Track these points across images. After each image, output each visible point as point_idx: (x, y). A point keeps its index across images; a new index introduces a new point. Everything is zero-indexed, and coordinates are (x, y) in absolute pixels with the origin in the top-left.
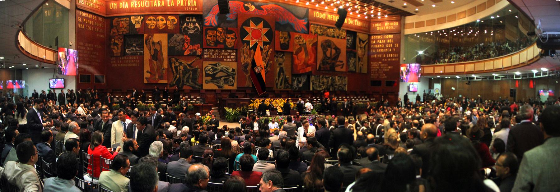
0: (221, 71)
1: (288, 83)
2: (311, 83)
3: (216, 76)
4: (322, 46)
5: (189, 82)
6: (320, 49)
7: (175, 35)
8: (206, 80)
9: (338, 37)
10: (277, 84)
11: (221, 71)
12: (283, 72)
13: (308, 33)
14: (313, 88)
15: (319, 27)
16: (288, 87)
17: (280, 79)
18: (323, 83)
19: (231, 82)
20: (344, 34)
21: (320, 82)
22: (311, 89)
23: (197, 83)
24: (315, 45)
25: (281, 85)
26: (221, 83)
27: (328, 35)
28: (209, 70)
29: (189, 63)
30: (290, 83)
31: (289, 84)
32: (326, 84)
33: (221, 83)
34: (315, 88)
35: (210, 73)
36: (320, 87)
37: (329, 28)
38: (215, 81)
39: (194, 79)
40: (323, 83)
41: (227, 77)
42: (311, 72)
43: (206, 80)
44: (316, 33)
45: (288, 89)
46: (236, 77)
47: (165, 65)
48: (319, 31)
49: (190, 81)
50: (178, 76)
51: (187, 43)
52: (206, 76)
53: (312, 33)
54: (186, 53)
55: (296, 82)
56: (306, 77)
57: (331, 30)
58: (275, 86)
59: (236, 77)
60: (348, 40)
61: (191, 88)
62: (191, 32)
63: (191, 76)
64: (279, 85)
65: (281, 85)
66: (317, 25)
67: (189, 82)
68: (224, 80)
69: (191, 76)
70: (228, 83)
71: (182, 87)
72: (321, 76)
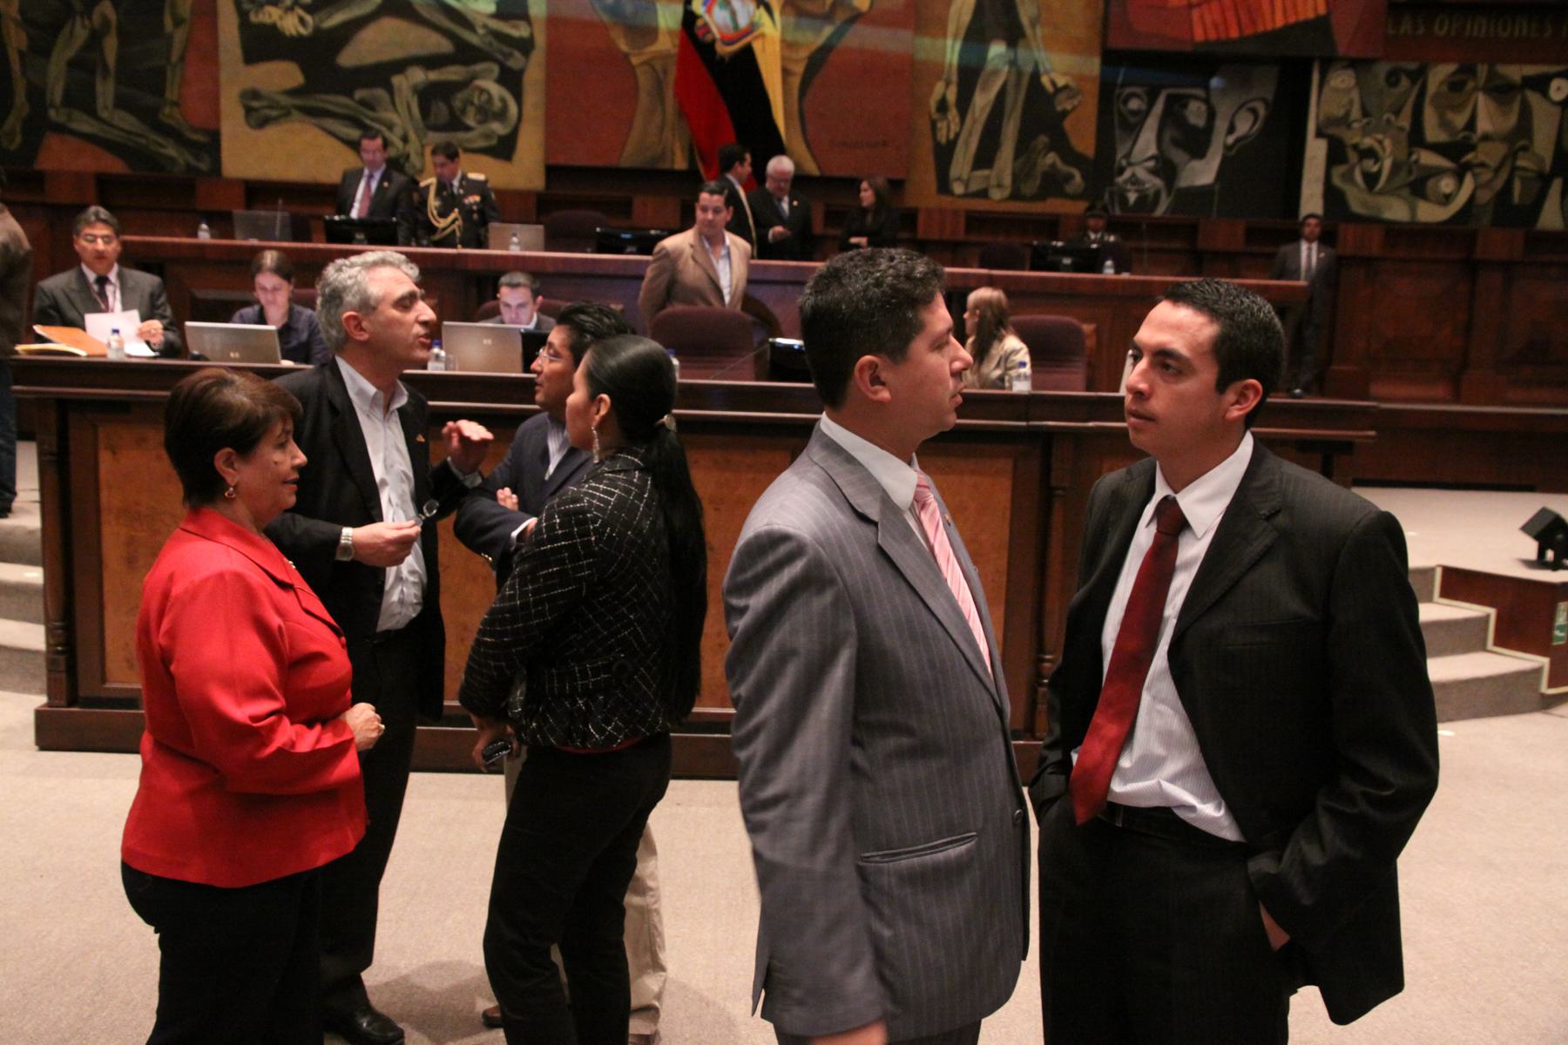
1: (1060, 143)
2: (1316, 151)
5: (91, 111)
10: (944, 154)
12: (1014, 36)
14: (1332, 196)
16: (1053, 185)
17: (982, 101)
18: (1457, 150)
19: (486, 114)
21: (1416, 137)
23: (168, 114)
25: (984, 159)
30: (1084, 140)
32: (1490, 154)
34: (1357, 200)
35: (291, 24)
36: (1418, 188)
38: (337, 102)
39: (144, 85)
40: (1457, 150)
41: (452, 73)
42: (1320, 26)
43: (254, 94)
45: (1054, 206)
46: (534, 74)
49: (105, 91)
55: (1147, 143)
56: (1265, 88)
58: (931, 178)
59: (534, 74)
61: (115, 165)
63: (111, 45)
65: (984, 159)
67: (91, 111)
68: (427, 95)
69: (111, 45)
70: (455, 124)
71: (32, 145)
72: (1439, 74)
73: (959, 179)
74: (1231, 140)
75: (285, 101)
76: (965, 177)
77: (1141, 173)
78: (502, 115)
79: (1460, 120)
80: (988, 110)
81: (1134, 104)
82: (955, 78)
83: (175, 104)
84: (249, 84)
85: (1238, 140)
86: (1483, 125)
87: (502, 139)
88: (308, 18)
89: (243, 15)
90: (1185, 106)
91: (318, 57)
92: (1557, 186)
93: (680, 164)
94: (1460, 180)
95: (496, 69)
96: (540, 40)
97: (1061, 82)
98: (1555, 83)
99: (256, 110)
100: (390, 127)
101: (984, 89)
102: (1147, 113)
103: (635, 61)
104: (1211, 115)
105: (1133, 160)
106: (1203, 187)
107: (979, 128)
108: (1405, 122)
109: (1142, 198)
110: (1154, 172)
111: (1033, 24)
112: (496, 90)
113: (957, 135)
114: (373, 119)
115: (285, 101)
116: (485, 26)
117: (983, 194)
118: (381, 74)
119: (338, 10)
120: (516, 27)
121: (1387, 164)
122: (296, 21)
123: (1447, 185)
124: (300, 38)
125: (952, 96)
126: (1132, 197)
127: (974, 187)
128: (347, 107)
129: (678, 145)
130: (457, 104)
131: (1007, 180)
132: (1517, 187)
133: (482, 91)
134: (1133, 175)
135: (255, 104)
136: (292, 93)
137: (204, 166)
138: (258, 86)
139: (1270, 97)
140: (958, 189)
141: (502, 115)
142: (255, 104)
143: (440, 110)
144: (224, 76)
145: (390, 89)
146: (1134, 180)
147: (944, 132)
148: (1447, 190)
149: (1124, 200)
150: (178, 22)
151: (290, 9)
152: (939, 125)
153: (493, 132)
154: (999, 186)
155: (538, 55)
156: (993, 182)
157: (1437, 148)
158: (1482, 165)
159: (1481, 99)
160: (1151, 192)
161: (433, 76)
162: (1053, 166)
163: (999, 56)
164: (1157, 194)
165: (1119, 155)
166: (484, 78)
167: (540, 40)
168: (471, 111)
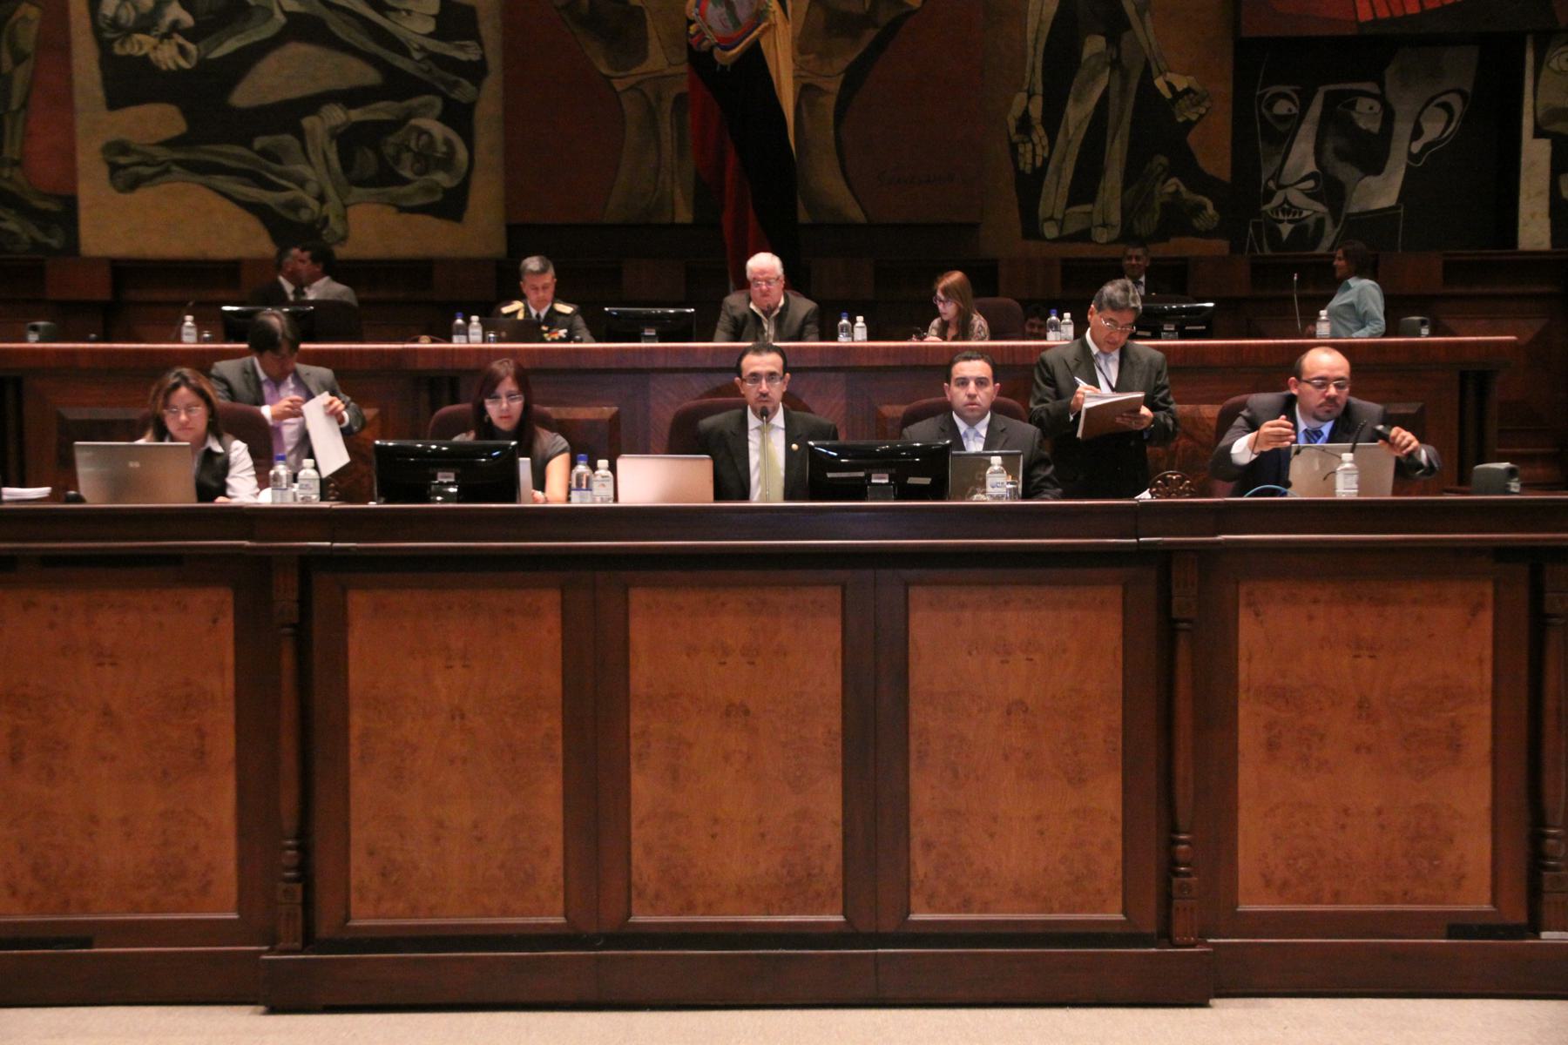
0: (302, 28)
1: (1184, 165)
3: (242, 97)
8: (116, 150)
10: (1030, 186)
11: (302, 28)
16: (1177, 220)
17: (1077, 114)
19: (427, 160)
25: (1084, 188)
26: (311, 173)
28: (146, 23)
30: (1216, 160)
31: (1200, 181)
33: (311, 173)
35: (167, 56)
41: (380, 111)
43: (122, 148)
46: (489, 102)
52: (116, 100)
55: (1302, 156)
59: (489, 102)
64: (1053, 198)
65: (1084, 188)
68: (349, 140)
70: (386, 177)
73: (1051, 218)
74: (1416, 147)
75: (163, 154)
76: (1059, 216)
77: (1296, 197)
78: (447, 163)
80: (1085, 126)
81: (1282, 107)
82: (1039, 88)
83: (16, 163)
84: (114, 135)
85: (1427, 146)
87: (446, 191)
88: (191, 47)
89: (104, 47)
90: (1352, 106)
91: (203, 95)
93: (684, 216)
95: (438, 103)
96: (494, 62)
97: (1181, 84)
99: (125, 167)
100: (302, 183)
101: (1077, 100)
102: (1300, 118)
103: (618, 86)
104: (1388, 117)
105: (1283, 181)
106: (1383, 217)
107: (1075, 150)
109: (1300, 230)
110: (1312, 195)
111: (1140, 13)
112: (438, 130)
113: (1046, 161)
114: (281, 175)
115: (163, 154)
116: (422, 49)
117: (1084, 236)
118: (287, 115)
119: (229, 37)
120: (462, 48)
122: (175, 51)
124: (180, 68)
125: (1036, 110)
126: (1286, 229)
127: (1071, 228)
128: (240, 158)
129: (678, 191)
130: (389, 150)
131: (1116, 217)
133: (422, 132)
134: (1286, 201)
135: (122, 160)
136: (170, 144)
137: (54, 243)
138: (125, 137)
139: (1468, 89)
140: (1051, 231)
141: (447, 163)
142: (122, 160)
143: (367, 161)
144: (81, 124)
145: (300, 134)
146: (1288, 208)
147: (1029, 156)
149: (1274, 234)
150: (19, 58)
151: (167, 36)
152: (1021, 150)
153: (438, 184)
154: (1104, 225)
155: (492, 85)
156: (1097, 219)
160: (1311, 222)
161: (356, 115)
162: (1177, 192)
163: (1098, 55)
164: (1320, 223)
165: (1264, 177)
166: (423, 115)
167: (494, 62)
168: (407, 158)
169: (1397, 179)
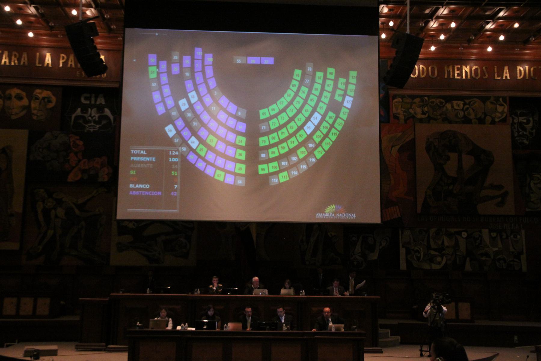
2: (403, 251)
4: (428, 149)
6: (423, 158)
7: (47, 135)
9: (481, 121)
13: (388, 122)
14: (408, 263)
15: (417, 100)
20: (503, 109)
21: (429, 247)
22: (403, 266)
24: (409, 148)
27: (446, 120)
29: (80, 201)
35: (131, 226)
36: (431, 260)
37: (449, 99)
44: (410, 118)
47: (17, 206)
48: (419, 110)
50: (51, 232)
51: (76, 153)
53: (396, 117)
54: (71, 178)
55: (358, 249)
57: (458, 105)
60: (521, 124)
62: (92, 128)
66: (413, 97)
72: (433, 231)
74: (381, 247)
79: (440, 242)
81: (354, 239)
86: (446, 244)
88: (136, 224)
92: (468, 259)
94: (442, 259)
97: (333, 234)
98: (463, 233)
108: (426, 244)
121: (422, 254)
123: (439, 259)
126: (355, 263)
132: (458, 259)
148: (439, 261)
157: (435, 250)
158: (448, 254)
159: (445, 238)
169: (377, 254)
